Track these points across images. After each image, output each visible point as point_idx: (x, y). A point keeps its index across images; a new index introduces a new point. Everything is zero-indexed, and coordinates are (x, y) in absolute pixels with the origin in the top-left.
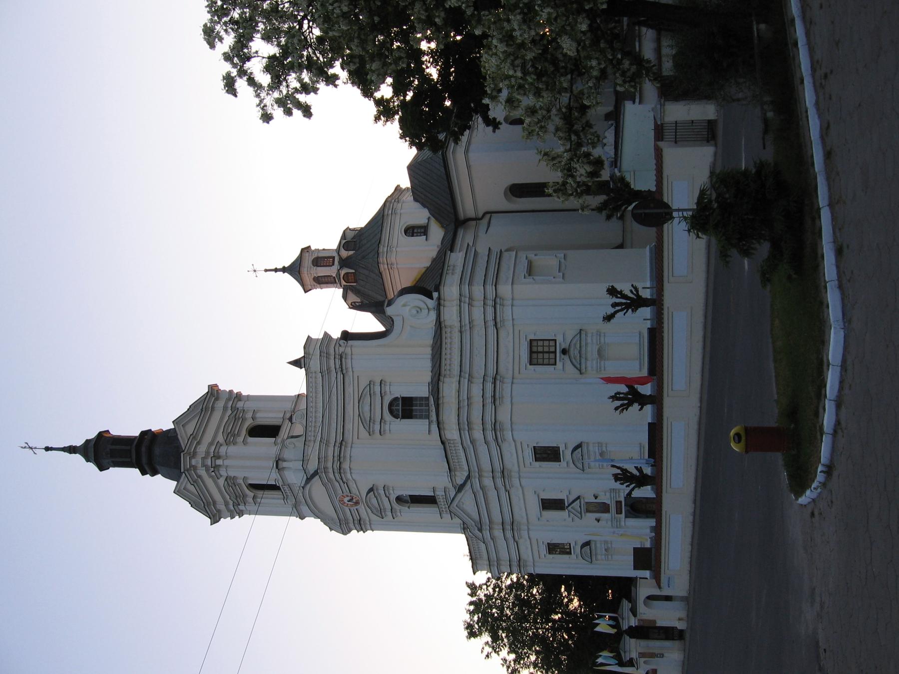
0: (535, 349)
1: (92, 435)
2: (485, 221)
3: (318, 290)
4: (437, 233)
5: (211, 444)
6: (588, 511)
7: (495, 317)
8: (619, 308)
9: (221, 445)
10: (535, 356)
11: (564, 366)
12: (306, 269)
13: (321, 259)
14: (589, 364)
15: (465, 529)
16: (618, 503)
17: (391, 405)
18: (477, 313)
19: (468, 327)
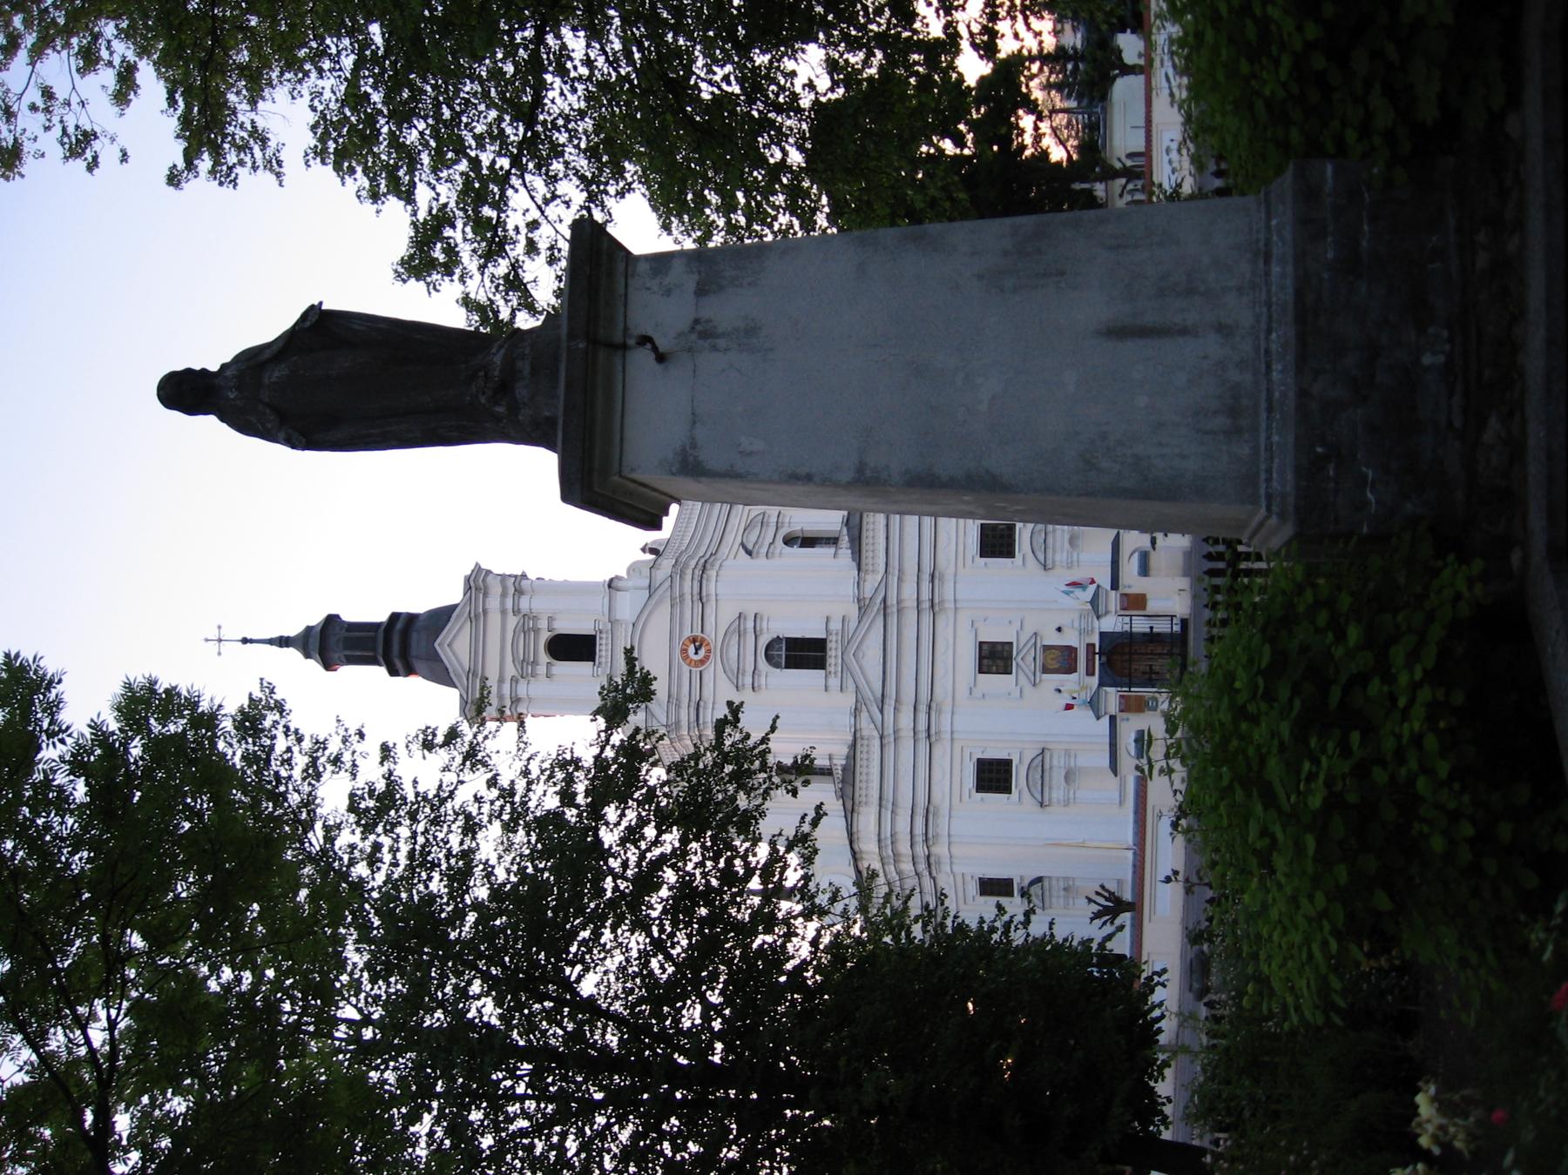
6: (1045, 670)
16: (1090, 646)
17: (769, 647)
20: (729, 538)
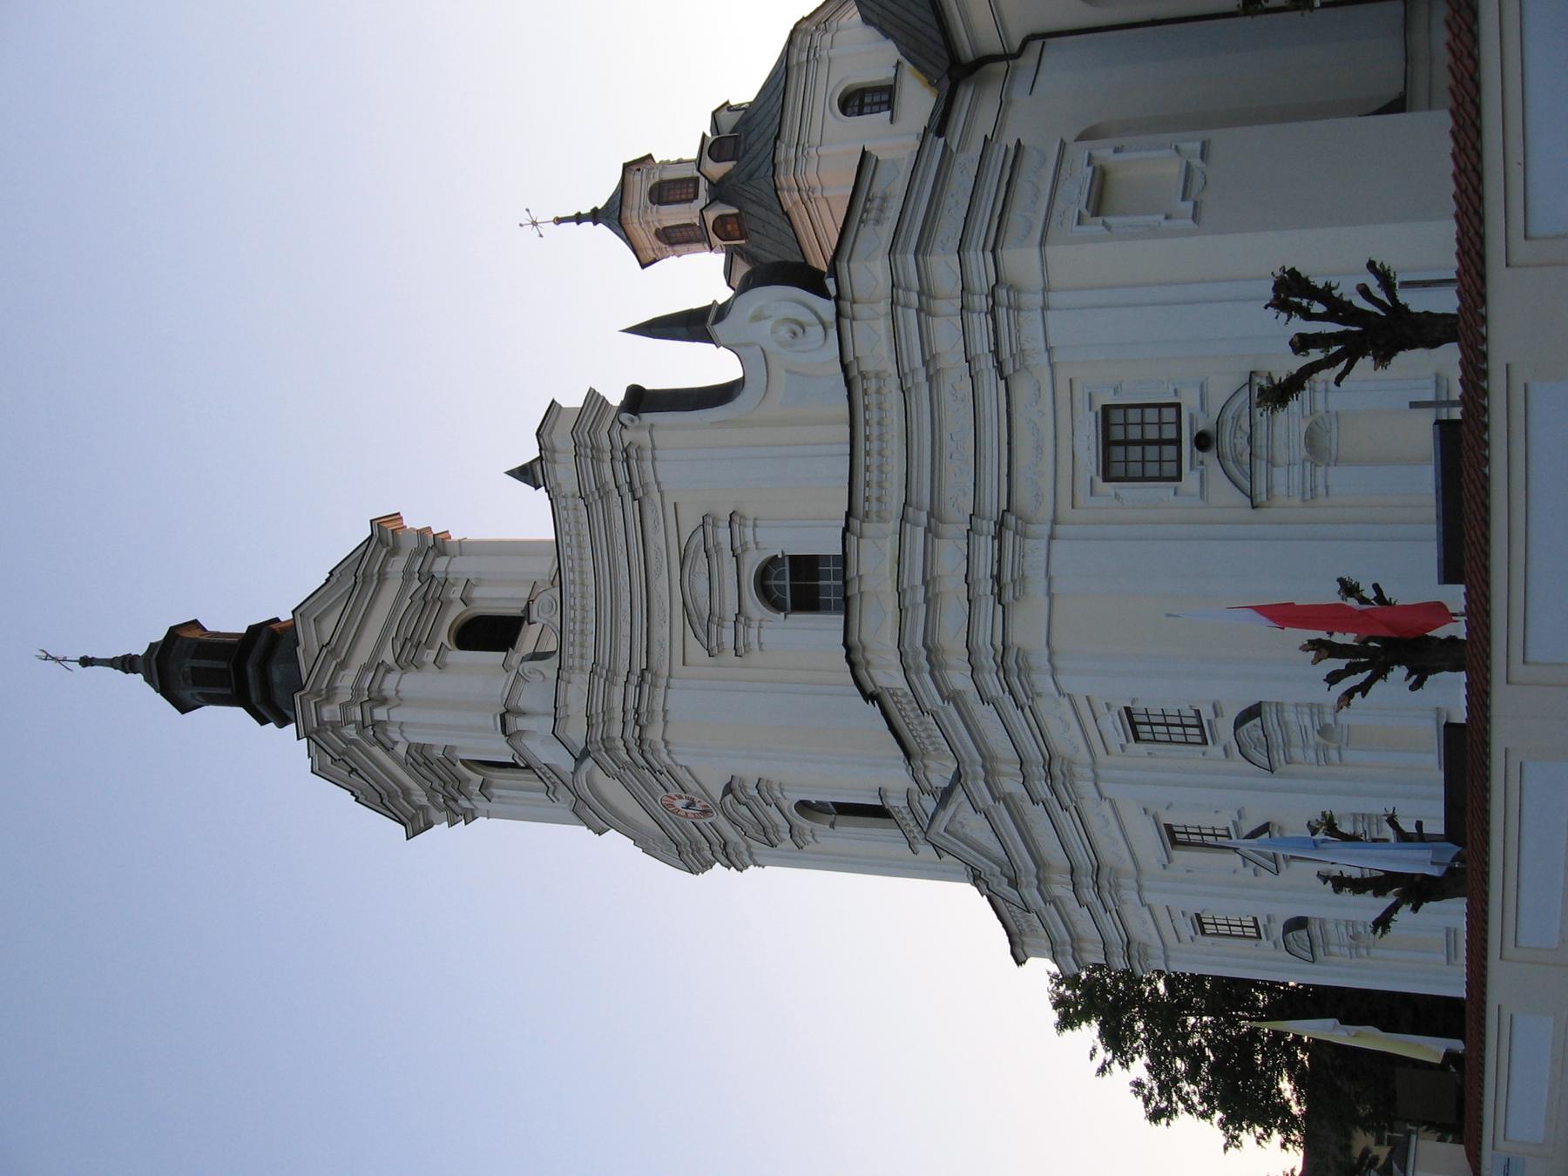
0: (1117, 433)
1: (159, 636)
2: (1029, 60)
3: (673, 259)
4: (918, 101)
5: (365, 668)
7: (996, 344)
8: (1316, 355)
9: (389, 670)
10: (1118, 453)
11: (1204, 487)
12: (635, 213)
13: (669, 188)
14: (1279, 474)
15: (977, 879)
18: (946, 334)
19: (922, 374)
20: (660, 585)
